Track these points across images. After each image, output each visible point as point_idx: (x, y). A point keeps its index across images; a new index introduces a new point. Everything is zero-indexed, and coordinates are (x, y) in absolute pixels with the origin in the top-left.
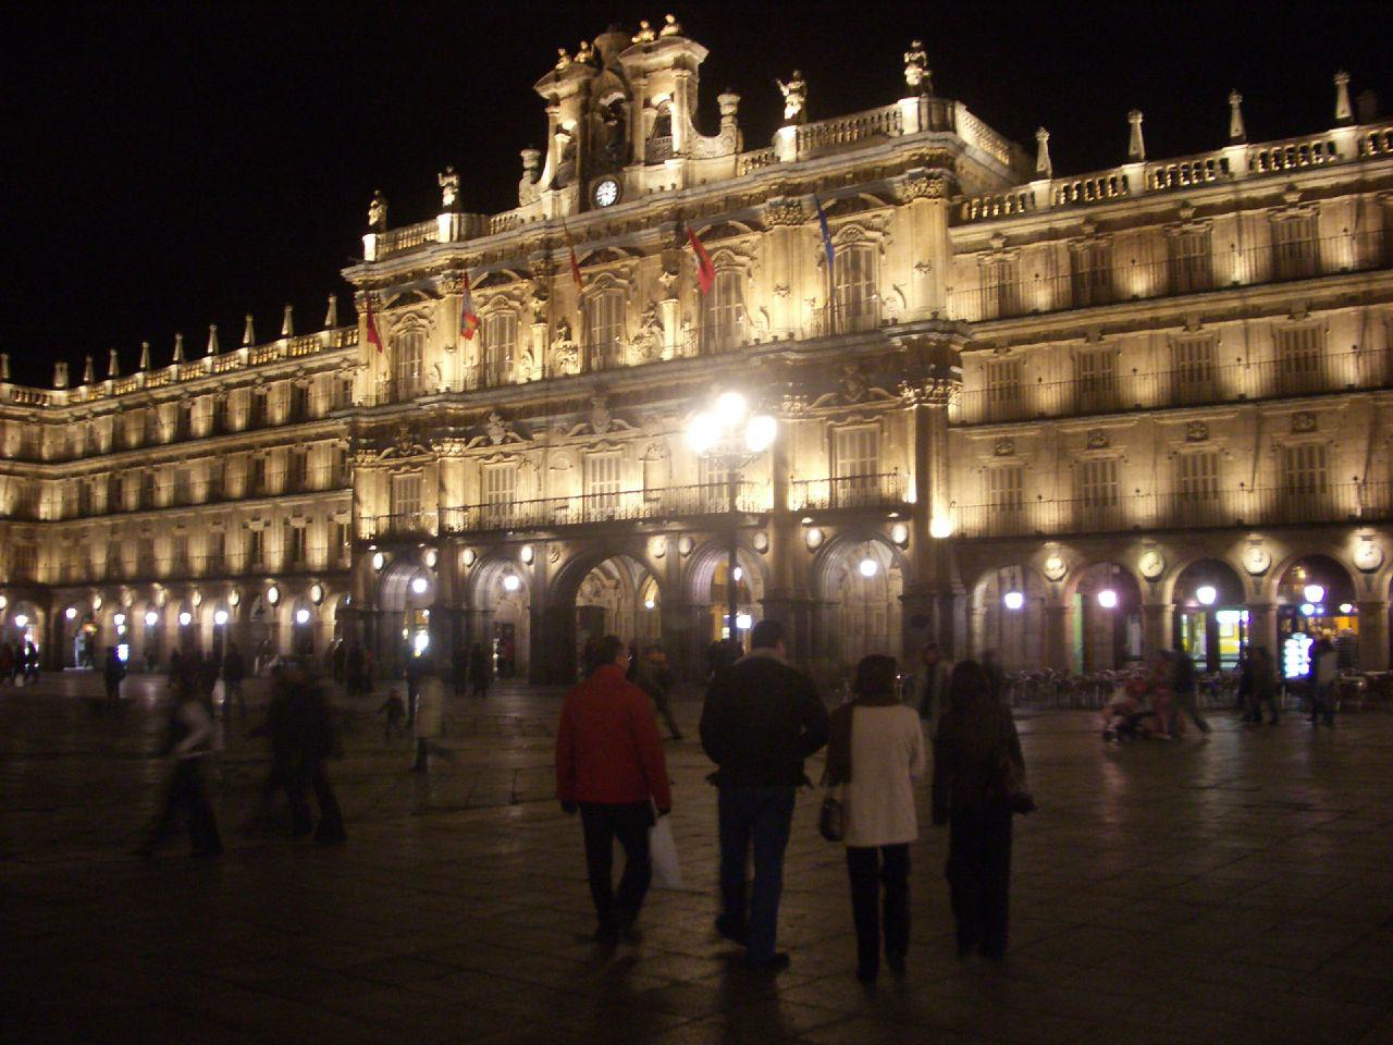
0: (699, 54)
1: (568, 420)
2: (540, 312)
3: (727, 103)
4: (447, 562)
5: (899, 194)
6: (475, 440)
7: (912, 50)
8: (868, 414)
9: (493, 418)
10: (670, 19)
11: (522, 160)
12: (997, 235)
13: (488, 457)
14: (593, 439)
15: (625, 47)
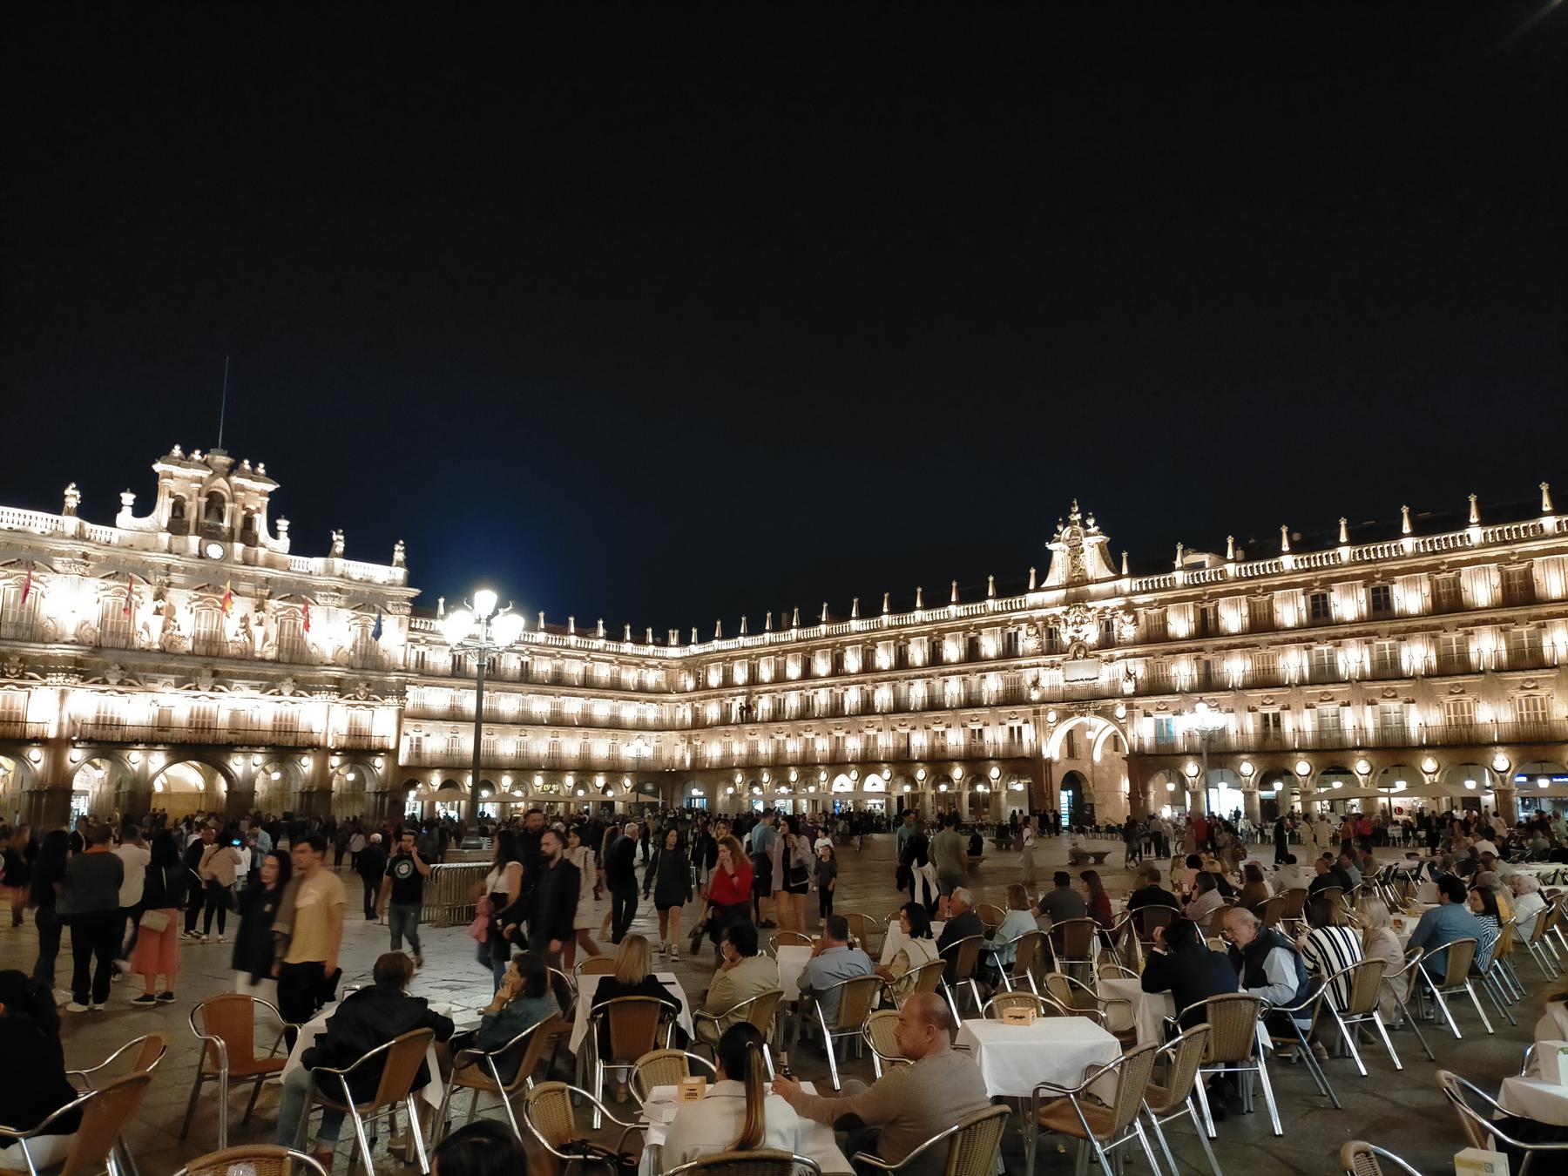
0: (271, 487)
1: (176, 679)
2: (162, 609)
3: (283, 524)
4: (57, 763)
5: (389, 609)
6: (94, 679)
7: (401, 545)
8: (367, 706)
9: (117, 667)
10: (262, 465)
11: (121, 498)
12: (423, 638)
13: (104, 691)
14: (197, 693)
15: (233, 469)
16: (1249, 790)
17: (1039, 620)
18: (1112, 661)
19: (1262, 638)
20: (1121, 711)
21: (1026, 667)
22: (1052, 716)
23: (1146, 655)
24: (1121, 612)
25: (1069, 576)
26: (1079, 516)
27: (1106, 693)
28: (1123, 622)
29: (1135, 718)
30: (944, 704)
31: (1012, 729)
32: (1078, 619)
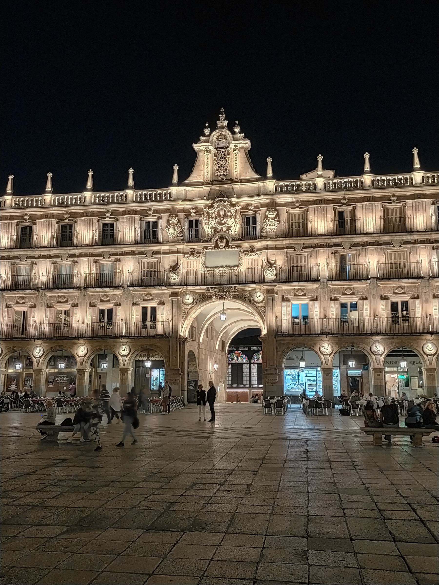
16: (380, 367)
17: (180, 211)
18: (253, 251)
19: (397, 238)
20: (259, 297)
21: (165, 253)
22: (189, 299)
23: (287, 248)
24: (264, 209)
25: (213, 174)
26: (226, 123)
27: (245, 279)
28: (266, 217)
29: (275, 303)
30: (71, 282)
31: (145, 310)
32: (222, 213)
